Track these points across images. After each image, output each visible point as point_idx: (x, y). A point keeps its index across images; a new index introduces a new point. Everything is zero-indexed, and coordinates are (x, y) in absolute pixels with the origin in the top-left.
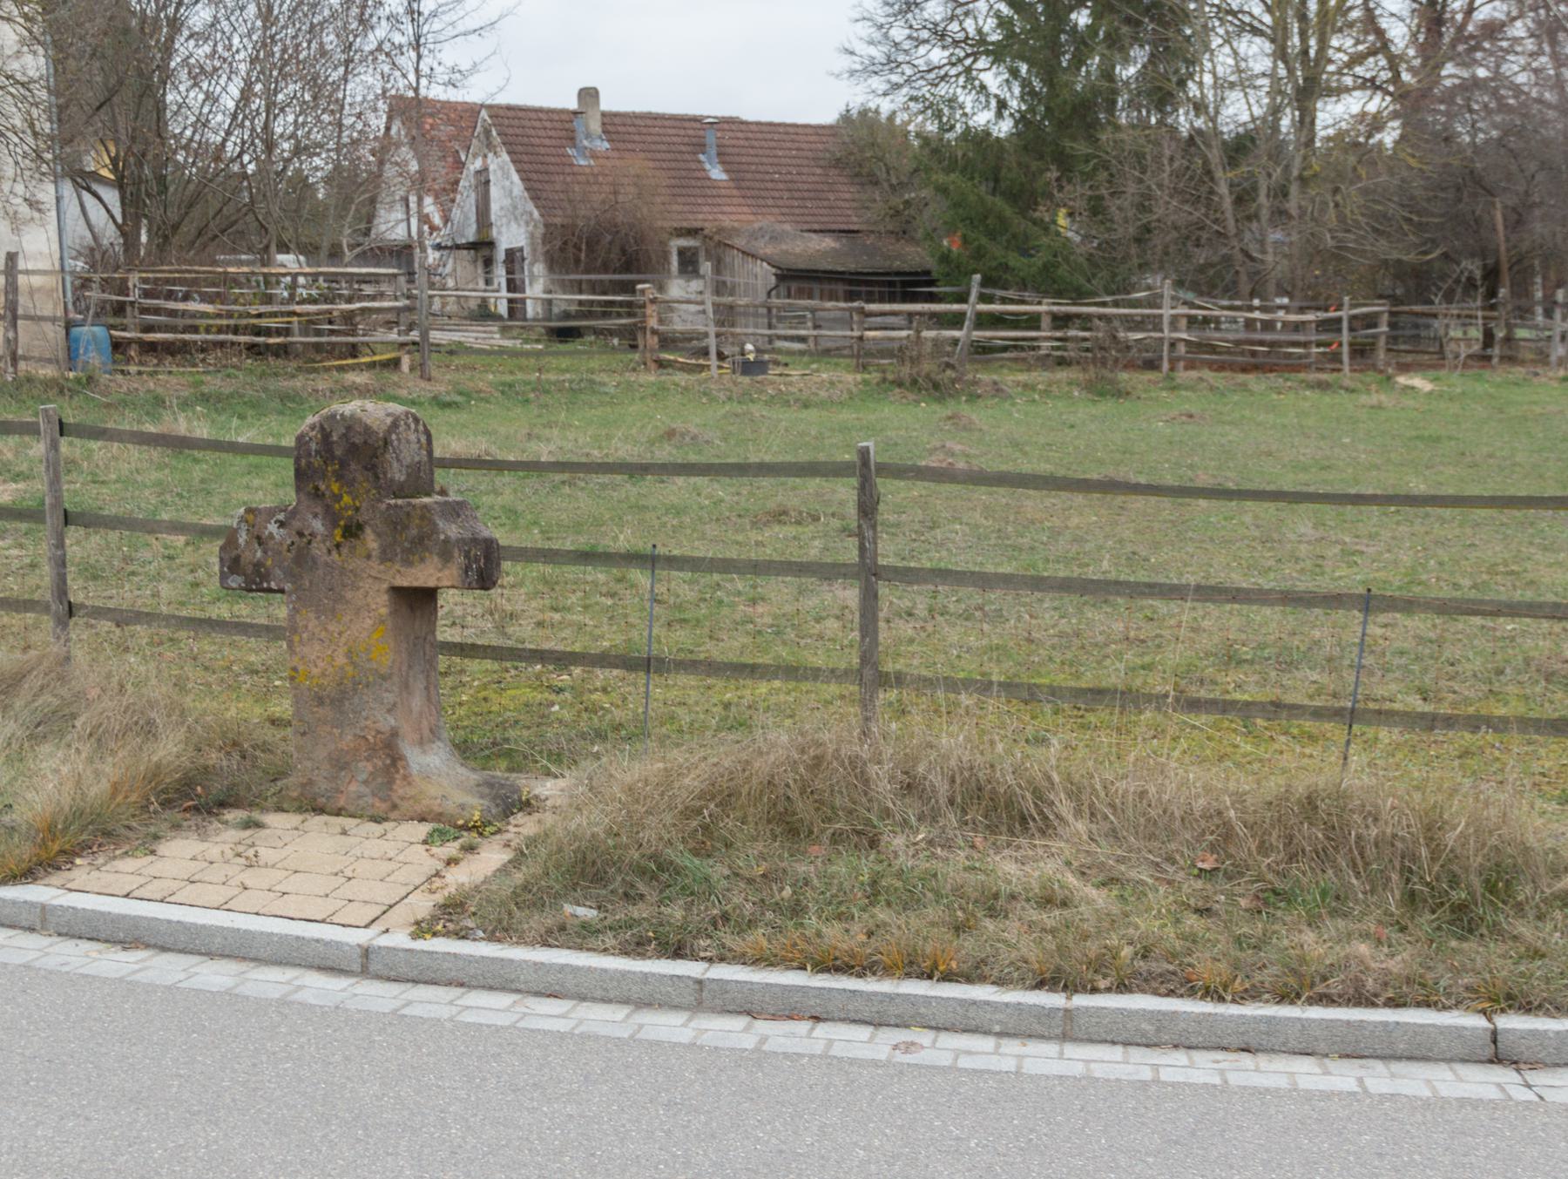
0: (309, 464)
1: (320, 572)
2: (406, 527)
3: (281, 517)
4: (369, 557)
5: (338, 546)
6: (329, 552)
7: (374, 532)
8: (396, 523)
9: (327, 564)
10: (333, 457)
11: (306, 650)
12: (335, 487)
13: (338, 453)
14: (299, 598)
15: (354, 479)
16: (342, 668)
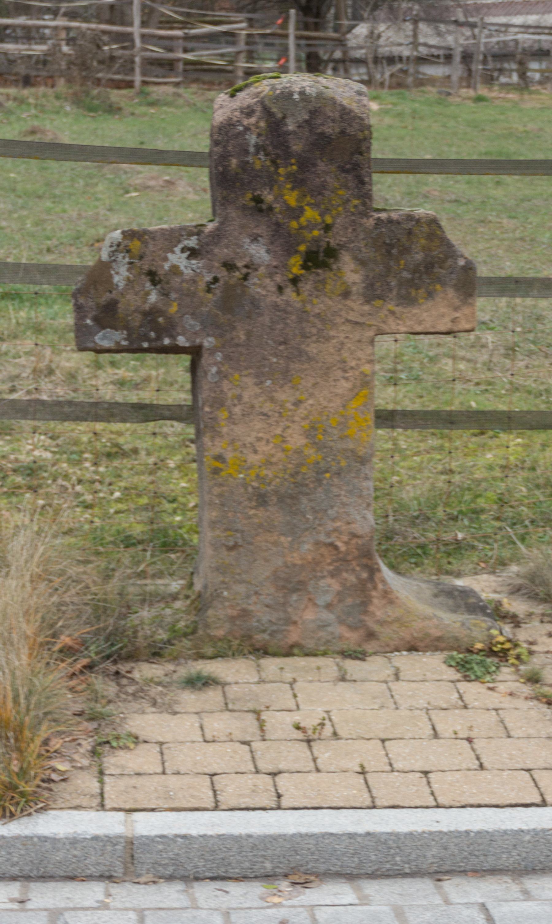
0: (244, 166)
1: (266, 319)
2: (406, 250)
3: (192, 242)
4: (346, 294)
5: (295, 281)
6: (280, 289)
7: (355, 258)
8: (392, 246)
9: (276, 307)
10: (287, 154)
11: (239, 430)
12: (292, 198)
13: (297, 147)
14: (228, 358)
15: (324, 186)
16: (299, 452)
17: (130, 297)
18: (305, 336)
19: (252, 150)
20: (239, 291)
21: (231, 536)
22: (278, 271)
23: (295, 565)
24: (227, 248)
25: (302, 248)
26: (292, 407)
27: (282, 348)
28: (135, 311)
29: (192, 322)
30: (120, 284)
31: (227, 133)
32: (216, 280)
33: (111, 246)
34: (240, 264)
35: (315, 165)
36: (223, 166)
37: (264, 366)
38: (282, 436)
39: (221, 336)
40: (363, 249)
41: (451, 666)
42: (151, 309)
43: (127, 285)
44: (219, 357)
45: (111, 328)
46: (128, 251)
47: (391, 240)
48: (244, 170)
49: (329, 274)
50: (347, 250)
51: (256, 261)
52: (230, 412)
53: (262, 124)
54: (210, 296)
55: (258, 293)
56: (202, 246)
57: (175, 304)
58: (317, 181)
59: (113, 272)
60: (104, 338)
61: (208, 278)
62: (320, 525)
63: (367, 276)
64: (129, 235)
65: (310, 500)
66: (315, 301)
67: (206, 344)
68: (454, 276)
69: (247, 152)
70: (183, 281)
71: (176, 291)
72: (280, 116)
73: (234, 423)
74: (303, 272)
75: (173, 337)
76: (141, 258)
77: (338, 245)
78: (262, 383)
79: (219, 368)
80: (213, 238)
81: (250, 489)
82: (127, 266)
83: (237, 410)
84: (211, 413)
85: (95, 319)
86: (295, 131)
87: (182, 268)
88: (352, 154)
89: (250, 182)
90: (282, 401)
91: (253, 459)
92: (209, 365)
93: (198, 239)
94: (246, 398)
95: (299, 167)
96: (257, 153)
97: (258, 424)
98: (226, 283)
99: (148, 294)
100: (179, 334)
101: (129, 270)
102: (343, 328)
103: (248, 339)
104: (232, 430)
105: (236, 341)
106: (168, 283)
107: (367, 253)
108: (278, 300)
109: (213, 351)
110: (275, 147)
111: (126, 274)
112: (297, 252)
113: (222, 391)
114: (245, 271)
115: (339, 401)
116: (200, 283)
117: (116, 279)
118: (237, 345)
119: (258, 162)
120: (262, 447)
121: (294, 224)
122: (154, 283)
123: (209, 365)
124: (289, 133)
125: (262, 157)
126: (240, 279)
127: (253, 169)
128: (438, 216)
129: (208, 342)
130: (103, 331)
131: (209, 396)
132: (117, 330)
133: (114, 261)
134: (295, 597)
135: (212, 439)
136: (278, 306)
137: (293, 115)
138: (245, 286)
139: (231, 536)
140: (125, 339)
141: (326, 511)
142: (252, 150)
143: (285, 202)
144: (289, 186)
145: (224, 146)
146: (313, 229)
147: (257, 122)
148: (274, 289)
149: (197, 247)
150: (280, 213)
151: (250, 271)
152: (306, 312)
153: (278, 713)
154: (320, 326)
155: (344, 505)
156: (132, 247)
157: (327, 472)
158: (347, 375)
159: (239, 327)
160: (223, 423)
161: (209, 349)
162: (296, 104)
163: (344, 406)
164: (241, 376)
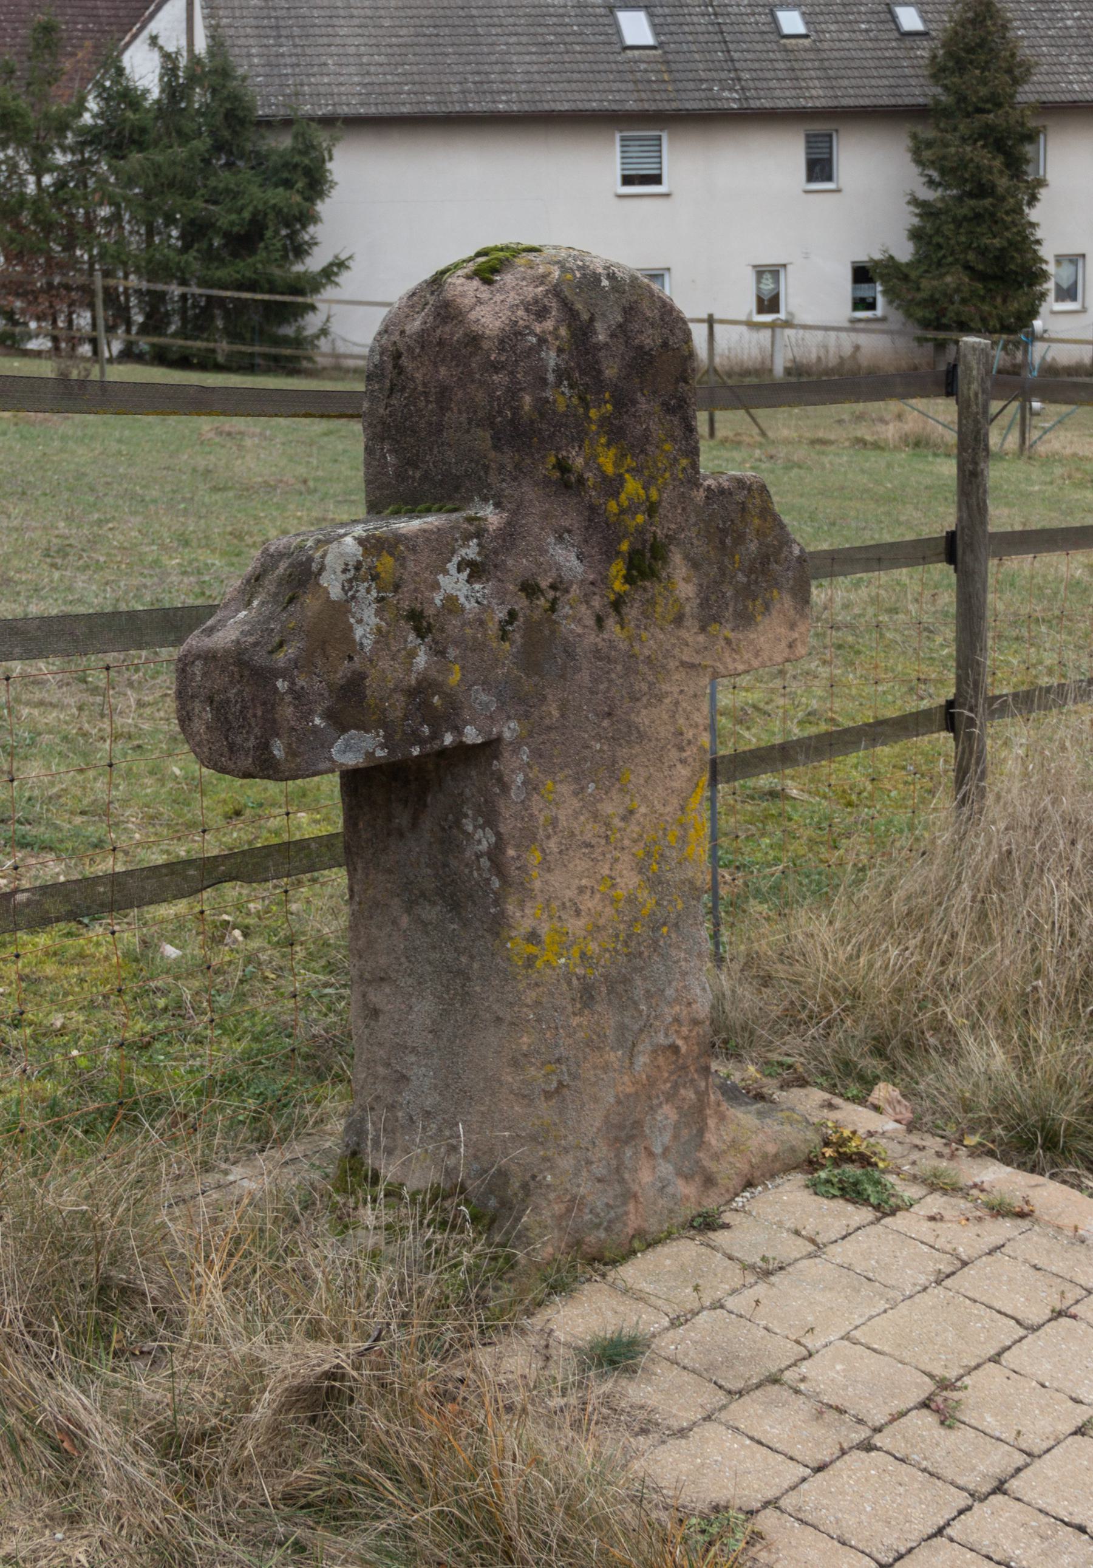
0: (542, 405)
1: (584, 677)
2: (740, 539)
3: (471, 551)
4: (679, 620)
5: (617, 605)
6: (600, 621)
7: (687, 557)
8: (724, 531)
9: (597, 654)
10: (599, 384)
11: (556, 879)
12: (607, 461)
13: (611, 371)
14: (537, 754)
15: (646, 436)
16: (631, 900)
17: (384, 664)
18: (634, 699)
19: (551, 377)
20: (547, 632)
21: (554, 1072)
22: (596, 590)
23: (628, 1096)
24: (525, 556)
25: (625, 547)
26: (622, 824)
27: (606, 723)
28: (394, 690)
29: (485, 698)
30: (365, 642)
31: (513, 348)
32: (512, 615)
33: (345, 571)
34: (544, 584)
35: (634, 402)
36: (511, 408)
37: (585, 759)
38: (611, 878)
39: (527, 716)
40: (695, 541)
41: (834, 1196)
42: (419, 682)
43: (377, 642)
44: (525, 756)
45: (357, 728)
46: (375, 578)
47: (724, 523)
48: (542, 415)
49: (658, 588)
50: (677, 545)
51: (567, 576)
52: (543, 851)
53: (563, 331)
54: (506, 645)
55: (572, 631)
56: (487, 556)
57: (457, 668)
58: (639, 430)
59: (352, 620)
60: (348, 748)
61: (501, 614)
62: (656, 1018)
63: (701, 585)
64: (374, 546)
65: (645, 979)
66: (645, 635)
67: (507, 735)
68: (790, 574)
69: (544, 381)
70: (464, 625)
71: (457, 644)
72: (585, 316)
73: (549, 870)
74: (627, 587)
75: (458, 730)
76: (397, 588)
77: (667, 536)
78: (583, 789)
79: (526, 775)
80: (504, 540)
81: (575, 982)
82: (374, 606)
83: (552, 845)
84: (519, 857)
85: (329, 715)
86: (607, 344)
87: (462, 600)
88: (677, 381)
89: (552, 436)
90: (608, 816)
91: (576, 926)
92: (513, 771)
93: (479, 545)
94: (563, 823)
95: (614, 406)
96: (559, 383)
97: (581, 865)
98: (528, 620)
99: (412, 654)
100: (466, 723)
101: (378, 613)
102: (677, 677)
103: (562, 716)
104: (547, 882)
105: (547, 722)
106: (442, 630)
107: (700, 548)
108: (598, 640)
109: (516, 746)
110: (583, 373)
111: (374, 620)
112: (618, 553)
113: (531, 815)
114: (551, 594)
115: (675, 802)
116: (490, 625)
117: (359, 632)
118: (549, 728)
119: (561, 399)
120: (589, 903)
121: (613, 506)
122: (421, 634)
123: (513, 771)
124: (598, 347)
125: (566, 391)
126: (546, 611)
127: (554, 412)
128: (768, 479)
129: (509, 730)
130: (346, 736)
131: (514, 827)
132: (367, 731)
133: (353, 597)
134: (629, 1152)
135: (521, 904)
136: (598, 651)
137: (604, 315)
138: (555, 622)
139: (554, 1072)
140: (382, 746)
141: (663, 991)
142: (551, 377)
143: (599, 468)
144: (603, 440)
145: (512, 373)
146: (636, 513)
147: (556, 329)
148: (591, 622)
149: (479, 559)
150: (594, 488)
151: (558, 594)
152: (633, 656)
153: (886, 1349)
154: (651, 678)
155: (684, 974)
156: (380, 569)
157: (665, 924)
158: (685, 755)
159: (550, 697)
160: (535, 874)
161: (511, 743)
162: (605, 295)
163: (682, 809)
164: (555, 782)
